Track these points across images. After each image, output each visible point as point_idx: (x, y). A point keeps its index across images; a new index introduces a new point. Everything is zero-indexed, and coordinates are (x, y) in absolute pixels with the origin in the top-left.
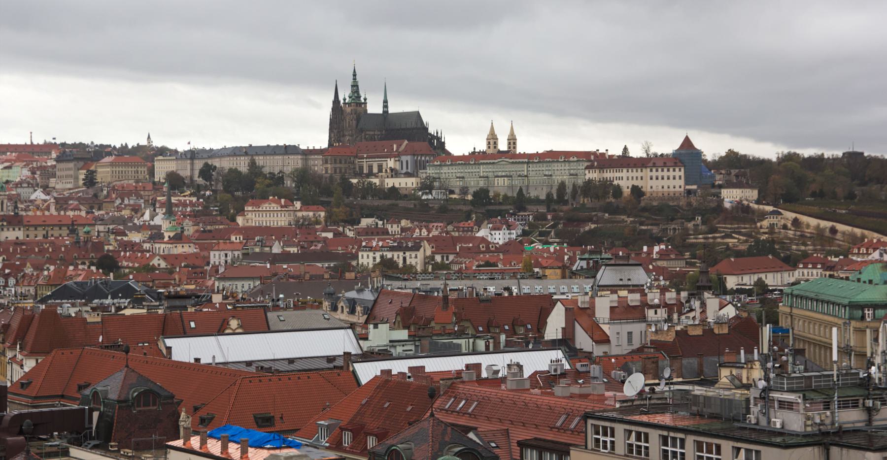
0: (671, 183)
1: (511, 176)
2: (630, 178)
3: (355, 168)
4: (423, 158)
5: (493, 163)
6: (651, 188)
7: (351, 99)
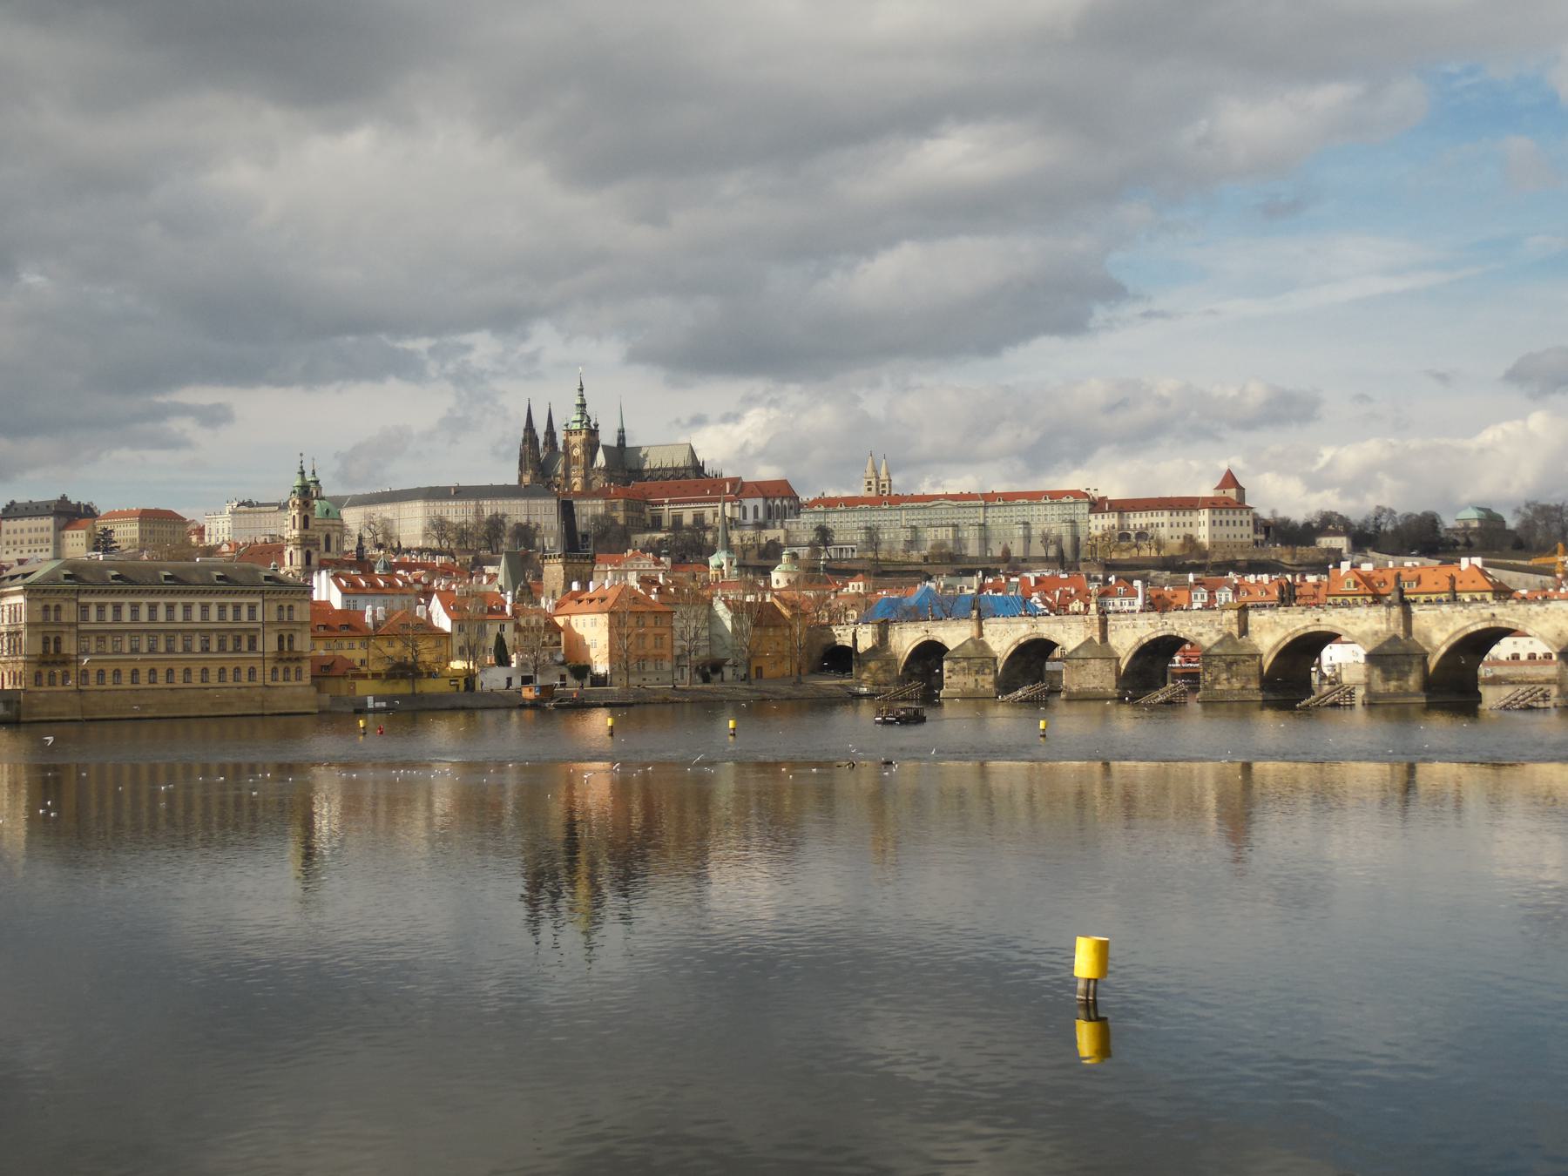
0: (1238, 530)
1: (954, 526)
2: (1175, 525)
3: (644, 520)
4: (785, 502)
5: (925, 507)
6: (1214, 536)
7: (579, 424)
